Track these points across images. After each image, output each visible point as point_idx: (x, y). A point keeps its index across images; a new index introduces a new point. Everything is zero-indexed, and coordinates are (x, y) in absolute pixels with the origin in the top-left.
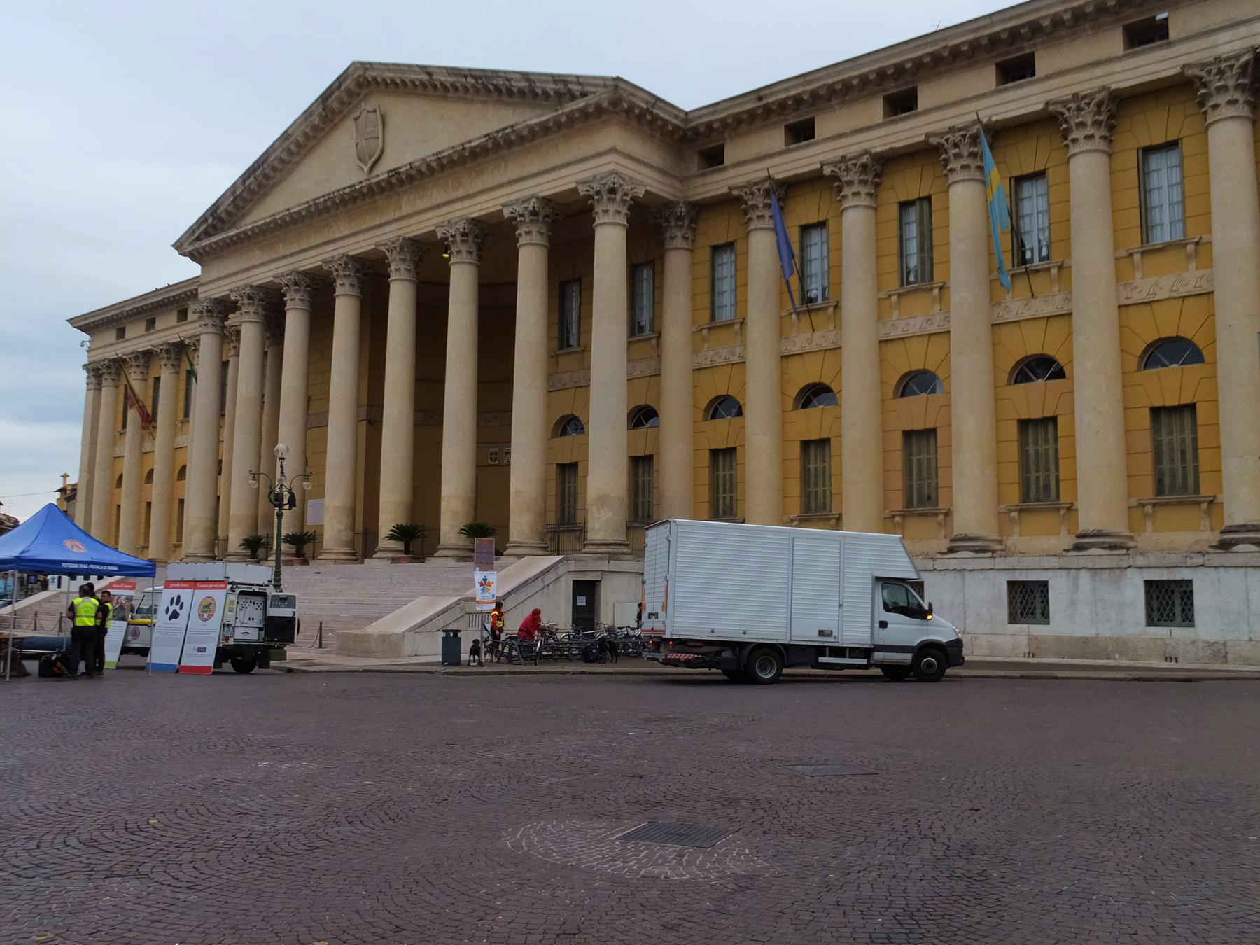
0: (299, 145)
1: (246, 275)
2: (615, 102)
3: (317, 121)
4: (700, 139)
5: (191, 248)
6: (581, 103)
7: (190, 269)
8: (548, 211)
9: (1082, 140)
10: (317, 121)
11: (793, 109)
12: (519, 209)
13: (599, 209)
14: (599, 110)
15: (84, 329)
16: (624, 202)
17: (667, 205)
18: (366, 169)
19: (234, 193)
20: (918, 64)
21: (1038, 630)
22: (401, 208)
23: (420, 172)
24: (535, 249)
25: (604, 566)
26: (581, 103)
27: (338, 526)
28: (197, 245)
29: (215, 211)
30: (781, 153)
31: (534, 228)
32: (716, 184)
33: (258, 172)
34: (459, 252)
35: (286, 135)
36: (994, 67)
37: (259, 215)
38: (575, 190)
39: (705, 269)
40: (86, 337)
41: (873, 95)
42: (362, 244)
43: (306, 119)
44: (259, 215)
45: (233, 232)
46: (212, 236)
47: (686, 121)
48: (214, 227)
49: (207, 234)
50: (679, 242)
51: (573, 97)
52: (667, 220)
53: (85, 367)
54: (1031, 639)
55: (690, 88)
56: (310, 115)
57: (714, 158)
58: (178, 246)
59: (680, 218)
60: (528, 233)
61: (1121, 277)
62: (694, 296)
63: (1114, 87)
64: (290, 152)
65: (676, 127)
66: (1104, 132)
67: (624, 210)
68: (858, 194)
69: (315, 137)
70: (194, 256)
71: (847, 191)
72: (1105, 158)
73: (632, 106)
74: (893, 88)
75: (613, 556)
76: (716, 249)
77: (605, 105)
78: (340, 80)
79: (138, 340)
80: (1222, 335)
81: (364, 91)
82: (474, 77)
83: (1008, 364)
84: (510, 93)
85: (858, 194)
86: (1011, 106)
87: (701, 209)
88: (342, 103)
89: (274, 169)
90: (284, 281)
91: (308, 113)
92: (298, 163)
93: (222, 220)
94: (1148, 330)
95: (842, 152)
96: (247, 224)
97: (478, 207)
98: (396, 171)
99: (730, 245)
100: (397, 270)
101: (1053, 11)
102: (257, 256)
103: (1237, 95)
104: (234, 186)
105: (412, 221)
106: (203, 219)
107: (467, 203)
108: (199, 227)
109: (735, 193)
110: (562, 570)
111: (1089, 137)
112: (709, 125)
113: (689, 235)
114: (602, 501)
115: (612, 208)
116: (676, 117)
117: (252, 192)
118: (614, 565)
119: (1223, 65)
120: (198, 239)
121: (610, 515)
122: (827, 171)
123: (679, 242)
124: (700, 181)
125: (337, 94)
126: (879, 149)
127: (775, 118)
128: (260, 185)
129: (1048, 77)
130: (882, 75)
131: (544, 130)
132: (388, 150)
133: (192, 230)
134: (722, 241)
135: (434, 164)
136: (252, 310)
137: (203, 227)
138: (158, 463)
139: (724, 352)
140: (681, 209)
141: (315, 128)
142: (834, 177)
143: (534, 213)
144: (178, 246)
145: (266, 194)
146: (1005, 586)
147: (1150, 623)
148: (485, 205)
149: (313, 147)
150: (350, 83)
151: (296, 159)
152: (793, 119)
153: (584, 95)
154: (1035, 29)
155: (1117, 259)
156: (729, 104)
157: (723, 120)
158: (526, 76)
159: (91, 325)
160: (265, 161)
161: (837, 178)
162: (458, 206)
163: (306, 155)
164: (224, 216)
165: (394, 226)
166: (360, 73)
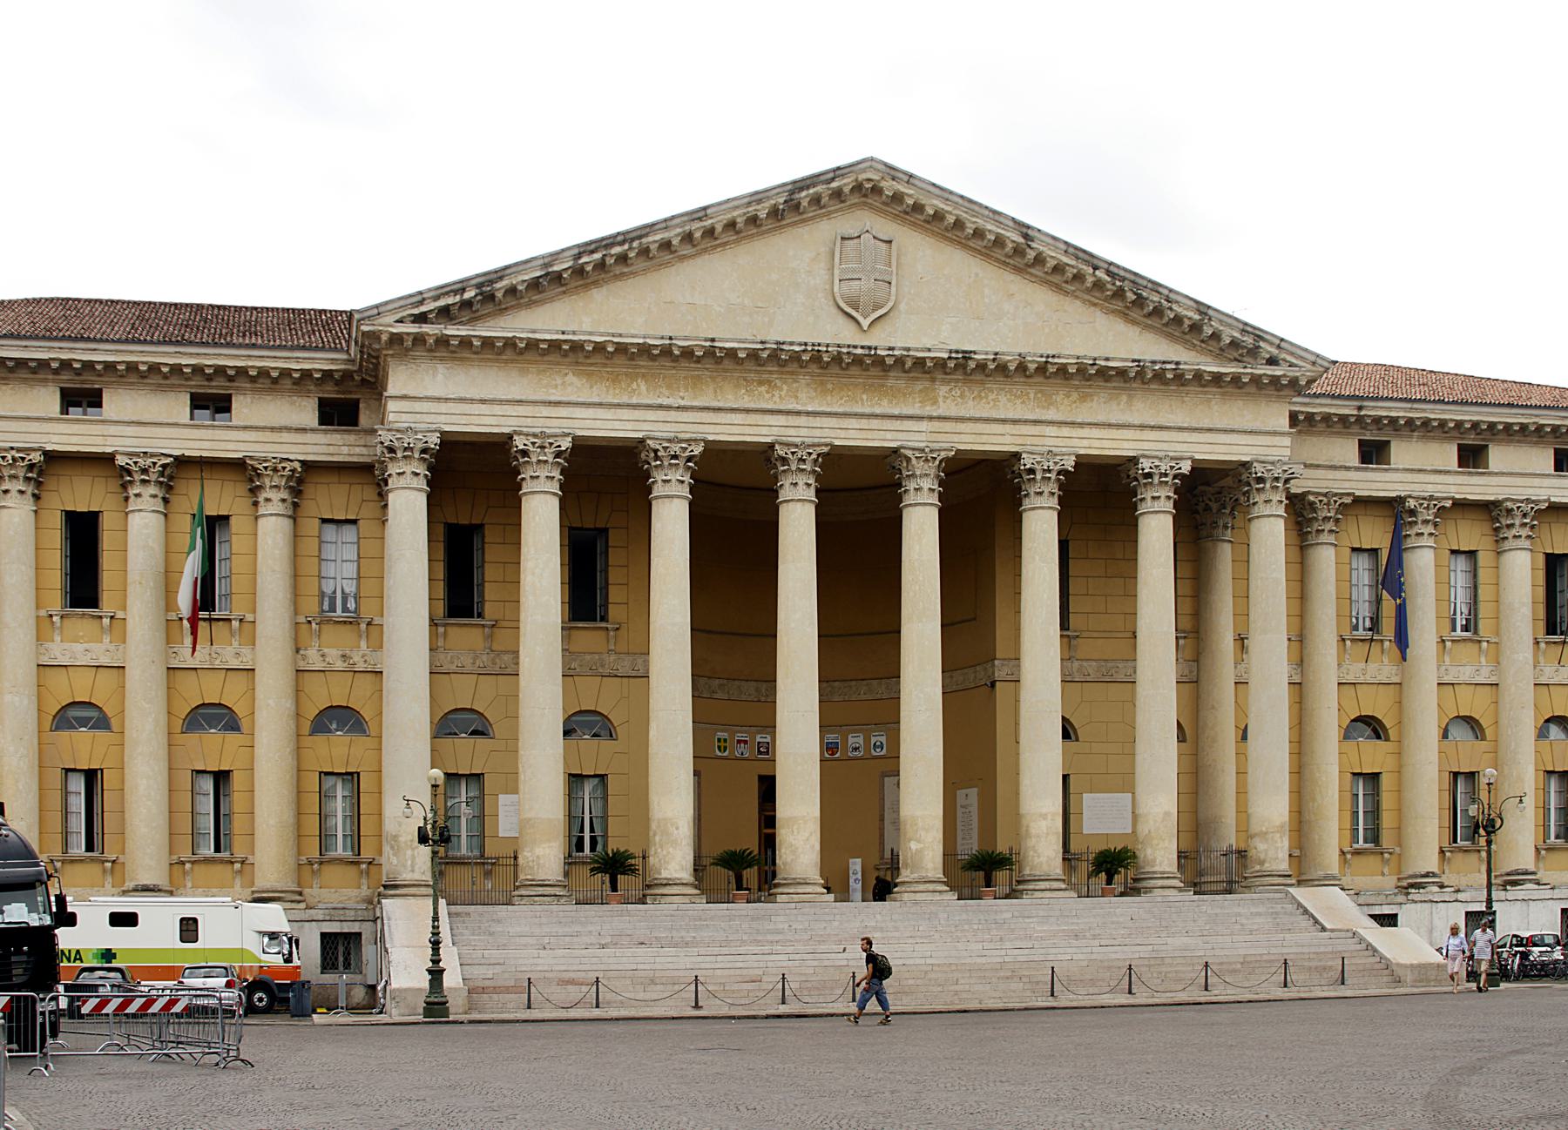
3: (762, 215)
10: (762, 215)
18: (865, 323)
19: (546, 265)
22: (935, 402)
33: (617, 250)
42: (852, 434)
43: (749, 203)
48: (467, 304)
49: (445, 313)
56: (759, 201)
69: (738, 233)
81: (855, 199)
82: (1108, 273)
90: (675, 448)
91: (758, 197)
92: (683, 258)
97: (1085, 443)
98: (967, 355)
102: (570, 385)
104: (556, 256)
105: (961, 427)
108: (436, 298)
120: (421, 318)
125: (819, 189)
131: (1217, 379)
133: (420, 298)
137: (450, 300)
141: (753, 220)
145: (596, 283)
148: (1106, 444)
149: (725, 244)
150: (846, 183)
151: (687, 250)
153: (1272, 361)
158: (1202, 309)
160: (640, 237)
162: (1051, 431)
163: (705, 250)
165: (924, 426)
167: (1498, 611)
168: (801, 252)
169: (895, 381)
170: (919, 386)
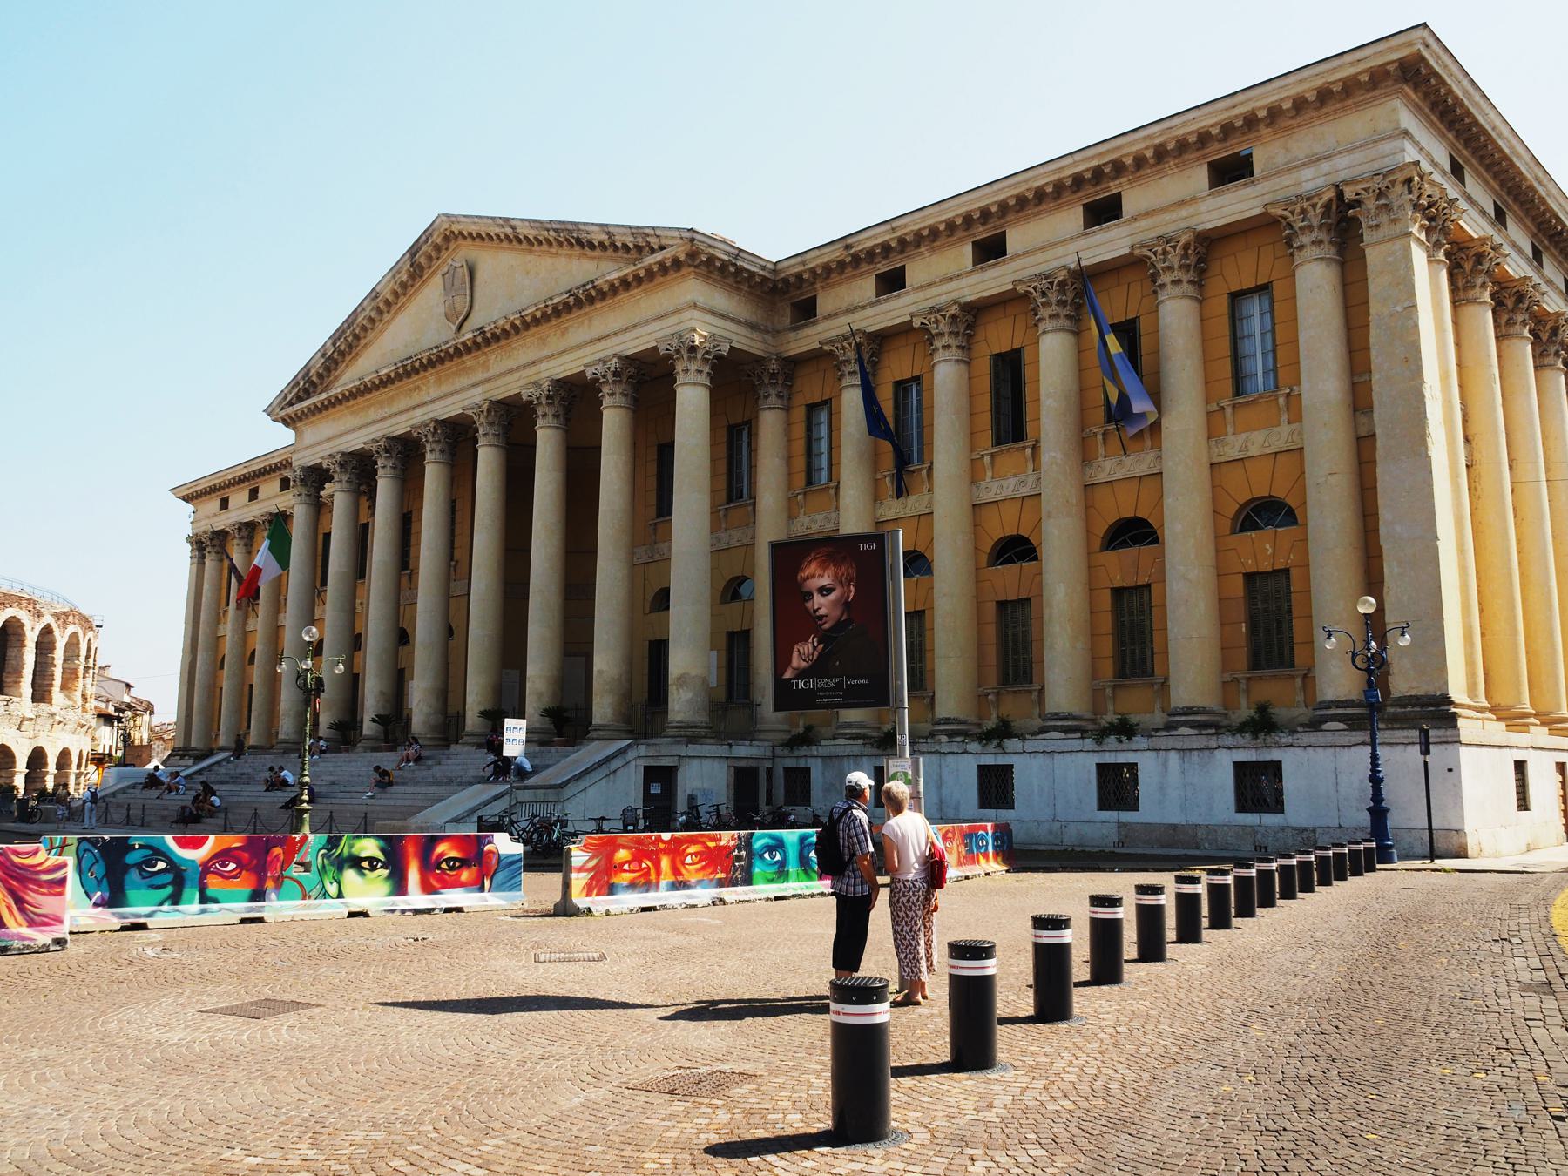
0: (388, 303)
1: (339, 441)
2: (693, 255)
3: (405, 278)
4: (786, 292)
5: (283, 413)
6: (658, 256)
7: (283, 437)
8: (632, 371)
9: (1169, 286)
10: (405, 278)
11: (883, 258)
12: (600, 368)
13: (679, 368)
14: (677, 264)
15: (187, 499)
16: (705, 360)
17: (758, 360)
18: (454, 328)
19: (323, 355)
20: (1004, 207)
21: (1127, 817)
23: (504, 330)
24: (618, 411)
25: (681, 750)
26: (658, 256)
27: (426, 709)
28: (290, 410)
29: (307, 373)
30: (872, 304)
31: (618, 389)
32: (807, 339)
34: (545, 415)
35: (374, 294)
36: (1081, 209)
37: (348, 378)
38: (655, 348)
39: (799, 431)
40: (189, 508)
41: (961, 240)
44: (348, 378)
45: (323, 396)
46: (305, 398)
47: (775, 271)
49: (300, 399)
50: (773, 401)
51: (653, 251)
52: (760, 377)
53: (189, 539)
54: (1121, 825)
55: (776, 236)
57: (806, 311)
58: (269, 411)
59: (773, 375)
60: (612, 394)
61: (1213, 431)
62: (789, 460)
63: (1200, 228)
64: (380, 312)
65: (764, 279)
66: (1191, 276)
67: (707, 369)
68: (949, 346)
70: (288, 422)
71: (938, 343)
72: (1195, 305)
73: (712, 259)
74: (982, 232)
75: (692, 740)
76: (812, 409)
77: (682, 258)
78: (427, 234)
79: (242, 509)
80: (1312, 495)
82: (556, 230)
83: (1101, 528)
84: (592, 246)
85: (949, 346)
86: (1098, 251)
87: (793, 366)
88: (430, 258)
89: (364, 328)
92: (388, 322)
93: (313, 384)
94: (1242, 490)
95: (930, 303)
96: (337, 390)
99: (826, 403)
100: (485, 435)
101: (1134, 149)
103: (1323, 236)
106: (294, 383)
107: (552, 363)
109: (826, 348)
110: (631, 755)
111: (1177, 282)
112: (799, 276)
113: (785, 393)
114: (683, 680)
115: (693, 367)
116: (763, 268)
117: (342, 354)
118: (693, 749)
119: (1305, 204)
120: (291, 404)
121: (690, 695)
122: (917, 323)
123: (773, 401)
124: (792, 335)
126: (968, 299)
127: (865, 267)
128: (350, 347)
129: (1134, 219)
130: (968, 220)
131: (625, 284)
132: (476, 307)
133: (283, 395)
134: (817, 399)
135: (518, 323)
136: (345, 478)
138: (259, 644)
139: (820, 517)
140: (773, 366)
141: (404, 285)
142: (924, 329)
143: (615, 374)
144: (269, 411)
146: (1094, 769)
147: (1100, 809)
152: (883, 267)
153: (662, 248)
154: (1118, 168)
155: (1209, 413)
156: (817, 252)
157: (813, 271)
159: (193, 496)
161: (927, 331)
164: (315, 379)
166: (446, 226)
167: (972, 422)
168: (431, 296)
169: (468, 360)
170: (482, 359)
